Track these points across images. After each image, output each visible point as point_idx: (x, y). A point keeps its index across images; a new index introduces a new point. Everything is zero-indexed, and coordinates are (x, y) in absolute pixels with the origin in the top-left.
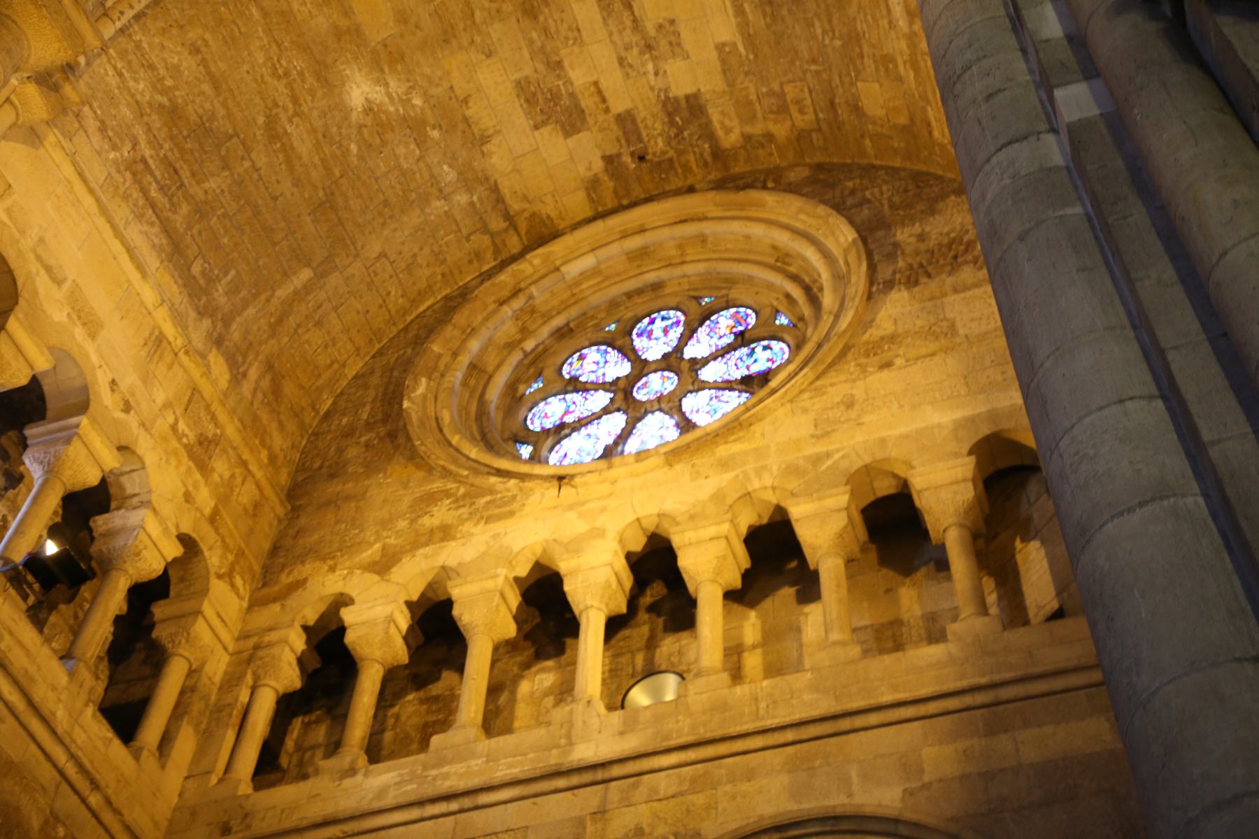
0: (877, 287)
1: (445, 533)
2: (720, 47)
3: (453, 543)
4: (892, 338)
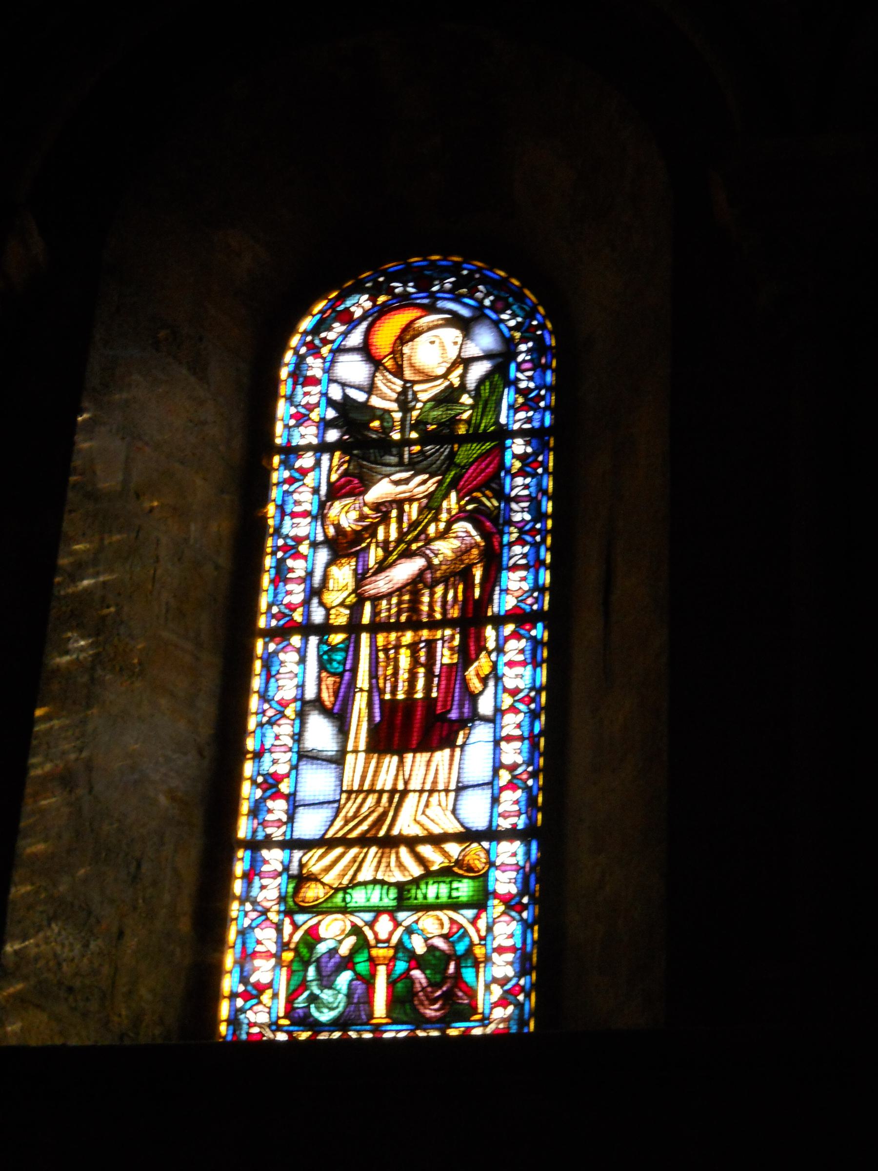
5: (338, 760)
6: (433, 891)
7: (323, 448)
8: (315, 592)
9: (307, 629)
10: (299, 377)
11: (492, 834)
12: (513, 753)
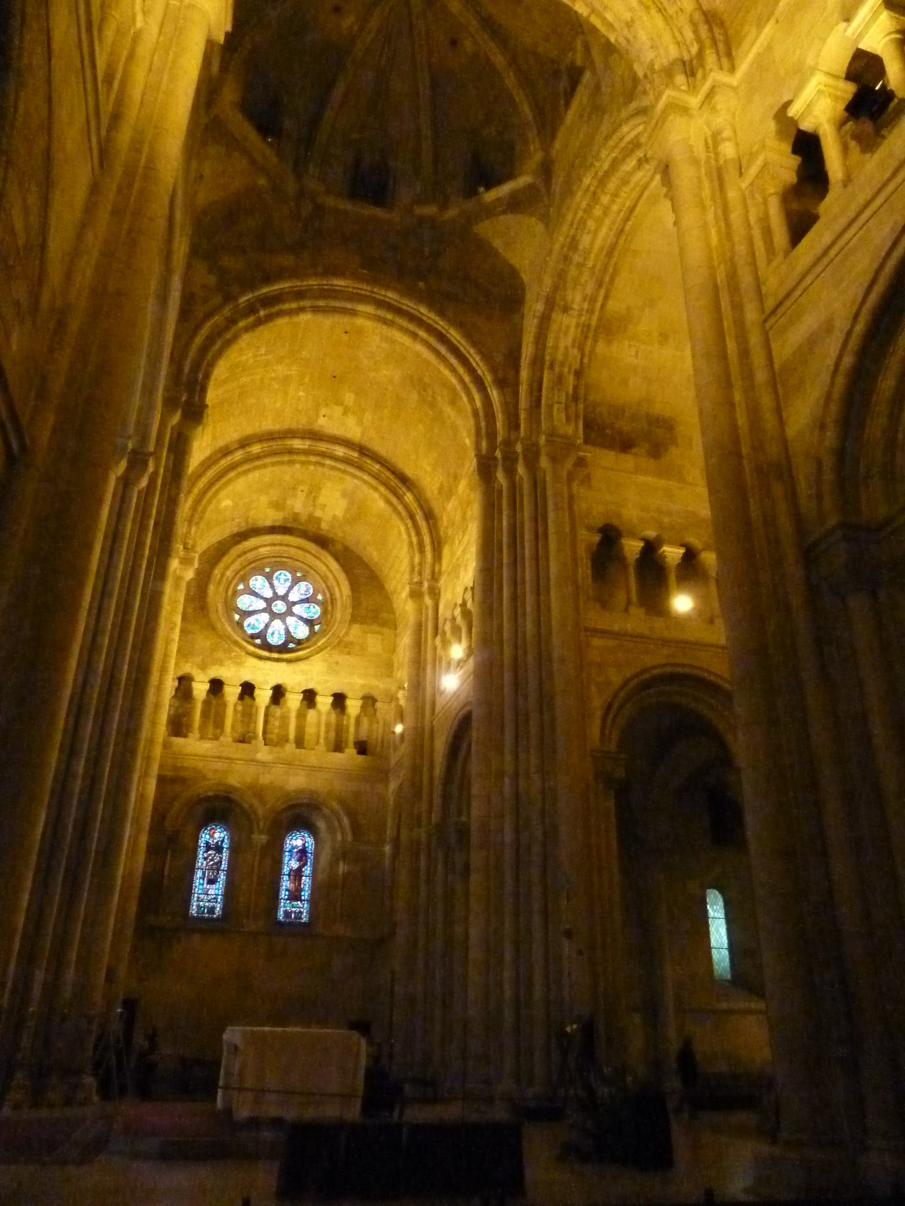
0: (354, 619)
1: (221, 663)
2: (335, 515)
3: (223, 667)
4: (352, 643)
5: (203, 885)
6: (212, 900)
7: (204, 847)
8: (202, 864)
9: (201, 869)
10: (202, 837)
11: (218, 895)
12: (221, 886)
